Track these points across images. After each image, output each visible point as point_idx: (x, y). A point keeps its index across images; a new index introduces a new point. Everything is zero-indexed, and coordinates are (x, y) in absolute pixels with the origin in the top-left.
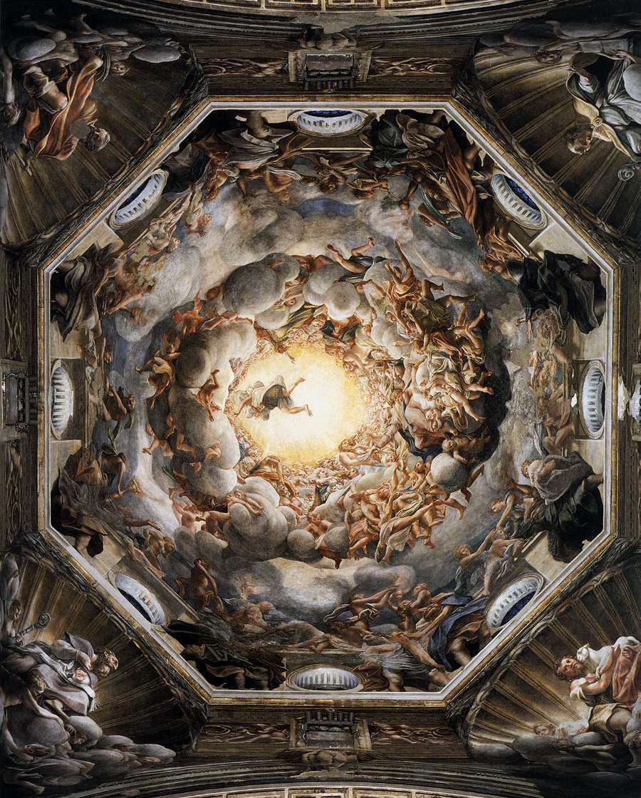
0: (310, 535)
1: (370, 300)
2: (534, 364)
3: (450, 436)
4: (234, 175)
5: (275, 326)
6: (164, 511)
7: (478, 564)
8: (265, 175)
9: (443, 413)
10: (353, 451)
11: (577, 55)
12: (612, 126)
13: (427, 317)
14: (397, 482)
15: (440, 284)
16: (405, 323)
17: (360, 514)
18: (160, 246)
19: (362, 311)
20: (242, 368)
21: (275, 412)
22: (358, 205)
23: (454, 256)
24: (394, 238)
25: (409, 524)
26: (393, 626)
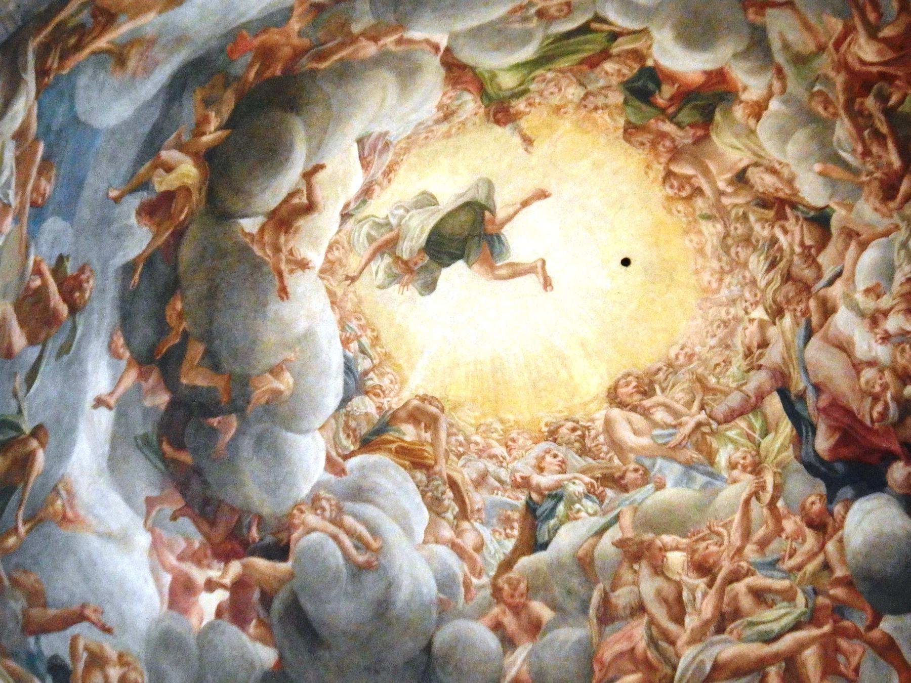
0: (492, 641)
1: (776, 45)
5: (500, 64)
10: (646, 413)
14: (746, 535)
16: (859, 130)
19: (747, 65)
21: (456, 276)
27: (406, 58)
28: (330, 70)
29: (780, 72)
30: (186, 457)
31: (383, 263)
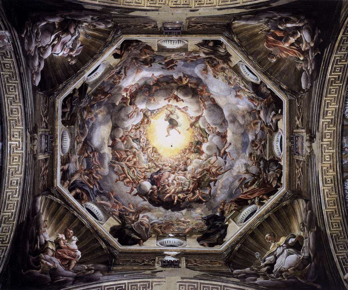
0: (120, 136)
1: (210, 159)
2: (185, 220)
3: (158, 188)
4: (258, 108)
5: (200, 123)
6: (132, 80)
7: (109, 199)
8: (258, 120)
9: (167, 186)
10: (152, 152)
11: (303, 238)
12: (276, 250)
13: (203, 180)
14: (141, 168)
15: (216, 185)
16: (201, 172)
17: (129, 155)
18: (231, 81)
20: (185, 111)
21: (167, 123)
22: (246, 154)
23: (226, 191)
24: (234, 168)
25: (125, 173)
26: (85, 167)
27: (200, 110)
28: (199, 100)
29: (206, 160)
30: (143, 89)
31: (169, 113)
